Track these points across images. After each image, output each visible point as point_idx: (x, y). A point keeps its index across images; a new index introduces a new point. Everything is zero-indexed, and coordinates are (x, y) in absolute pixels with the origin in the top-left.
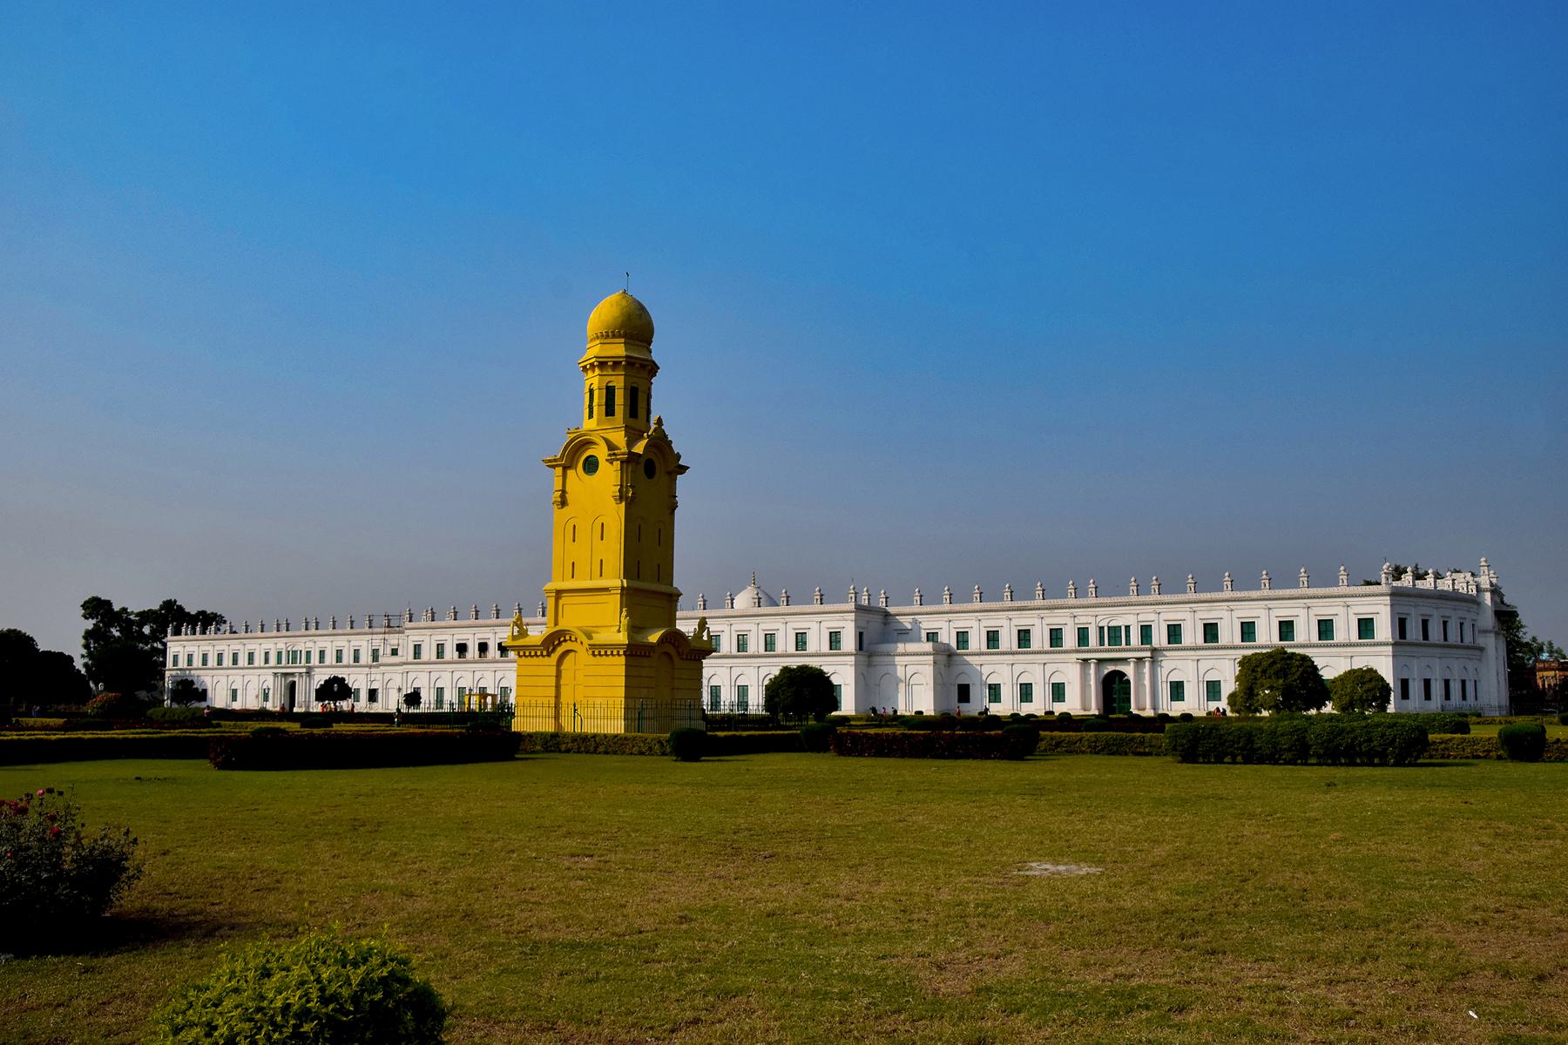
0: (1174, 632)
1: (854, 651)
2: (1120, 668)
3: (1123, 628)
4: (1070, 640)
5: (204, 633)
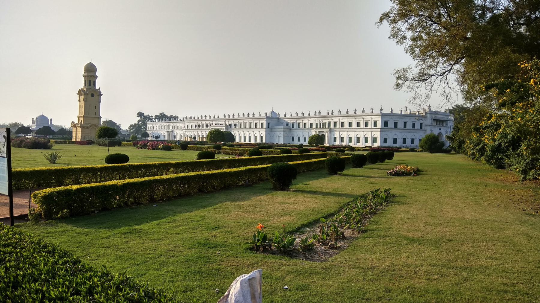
4: (314, 126)
5: (165, 121)
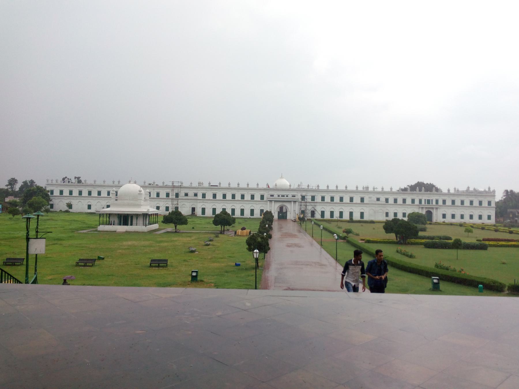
0: (444, 202)
1: (495, 206)
2: (430, 210)
4: (417, 202)
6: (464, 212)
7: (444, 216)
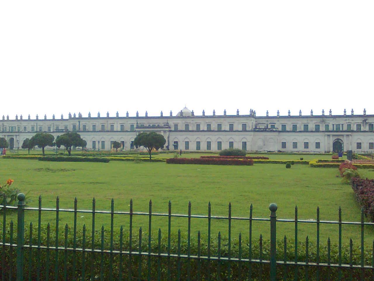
2: (341, 138)
3: (341, 125)
6: (319, 139)
7: (359, 145)
